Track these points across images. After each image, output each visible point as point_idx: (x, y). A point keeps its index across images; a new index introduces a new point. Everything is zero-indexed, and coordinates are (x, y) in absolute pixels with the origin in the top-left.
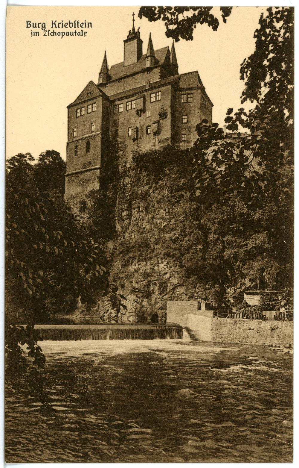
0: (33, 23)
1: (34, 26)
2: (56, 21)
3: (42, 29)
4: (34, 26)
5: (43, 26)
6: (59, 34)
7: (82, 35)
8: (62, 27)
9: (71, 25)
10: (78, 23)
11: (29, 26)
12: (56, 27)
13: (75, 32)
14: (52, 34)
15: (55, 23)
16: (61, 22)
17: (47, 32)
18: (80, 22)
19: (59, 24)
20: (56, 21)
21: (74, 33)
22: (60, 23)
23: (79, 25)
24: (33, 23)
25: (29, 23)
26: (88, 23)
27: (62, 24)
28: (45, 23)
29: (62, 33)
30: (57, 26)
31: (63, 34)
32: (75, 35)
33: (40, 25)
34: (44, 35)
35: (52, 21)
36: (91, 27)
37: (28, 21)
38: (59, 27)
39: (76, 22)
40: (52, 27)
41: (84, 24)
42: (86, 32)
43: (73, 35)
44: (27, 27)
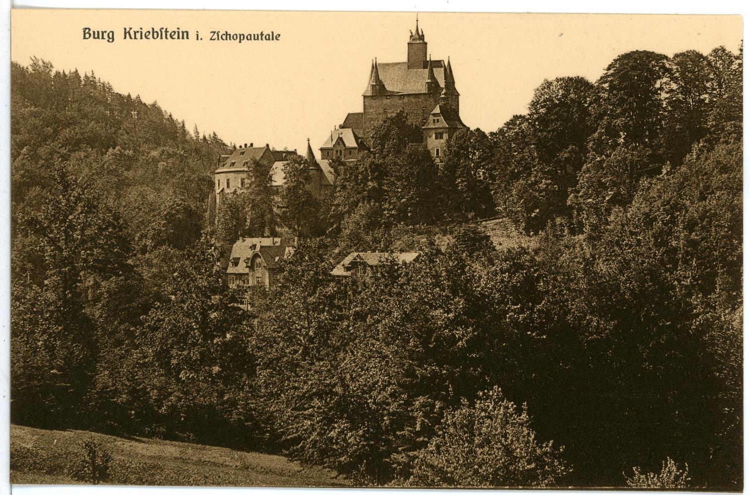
1: (96, 36)
3: (108, 41)
4: (96, 36)
5: (111, 36)
6: (235, 37)
7: (273, 39)
8: (141, 38)
9: (155, 36)
10: (166, 31)
11: (87, 36)
12: (131, 38)
13: (262, 34)
14: (224, 37)
15: (129, 32)
17: (216, 34)
18: (170, 31)
19: (135, 33)
20: (131, 29)
21: (260, 36)
22: (138, 32)
23: (168, 34)
24: (94, 32)
27: (141, 32)
28: (113, 32)
29: (240, 35)
30: (133, 36)
31: (242, 37)
32: (262, 39)
33: (105, 35)
34: (211, 39)
35: (125, 29)
36: (187, 38)
37: (86, 29)
38: (135, 38)
39: (163, 31)
40: (125, 38)
41: (177, 33)
42: (279, 35)
43: (258, 39)
44: (85, 38)
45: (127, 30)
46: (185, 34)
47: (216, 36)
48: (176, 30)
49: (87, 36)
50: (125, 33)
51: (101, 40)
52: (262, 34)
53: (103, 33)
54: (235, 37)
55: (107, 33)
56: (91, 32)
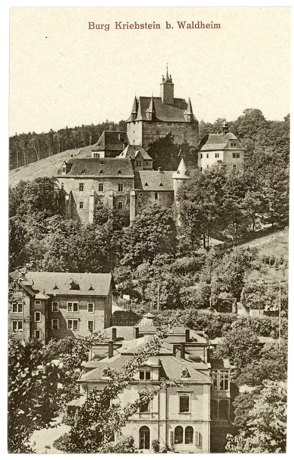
0: (96, 25)
2: (120, 22)
4: (98, 27)
8: (128, 28)
11: (92, 27)
15: (119, 25)
18: (148, 24)
19: (124, 25)
20: (120, 22)
22: (126, 25)
24: (96, 25)
25: (92, 24)
26: (157, 25)
27: (128, 25)
30: (122, 27)
33: (104, 27)
35: (116, 23)
37: (90, 23)
44: (90, 28)
45: (118, 24)
46: (158, 26)
50: (117, 26)
51: (100, 29)
53: (102, 25)
55: (105, 25)
56: (95, 25)
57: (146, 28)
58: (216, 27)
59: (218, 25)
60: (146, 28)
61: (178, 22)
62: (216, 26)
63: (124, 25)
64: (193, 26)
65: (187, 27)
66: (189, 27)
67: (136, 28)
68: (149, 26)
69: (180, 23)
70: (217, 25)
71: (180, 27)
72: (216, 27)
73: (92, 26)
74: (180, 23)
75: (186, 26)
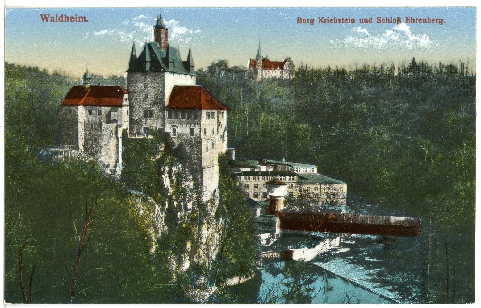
2: (322, 18)
9: (336, 20)
11: (300, 21)
16: (327, 19)
18: (344, 19)
19: (325, 20)
20: (322, 18)
23: (344, 20)
26: (352, 20)
27: (328, 20)
30: (323, 21)
35: (319, 18)
37: (298, 18)
47: (379, 20)
48: (348, 19)
49: (300, 21)
51: (307, 24)
52: (343, 19)
54: (395, 21)
57: (343, 22)
58: (81, 20)
59: (83, 19)
60: (343, 22)
61: (42, 15)
62: (81, 18)
63: (325, 20)
64: (57, 18)
65: (51, 21)
66: (53, 20)
67: (335, 22)
68: (345, 21)
69: (44, 16)
70: (82, 18)
71: (43, 20)
72: (81, 20)
73: (300, 20)
74: (44, 16)
75: (49, 19)
